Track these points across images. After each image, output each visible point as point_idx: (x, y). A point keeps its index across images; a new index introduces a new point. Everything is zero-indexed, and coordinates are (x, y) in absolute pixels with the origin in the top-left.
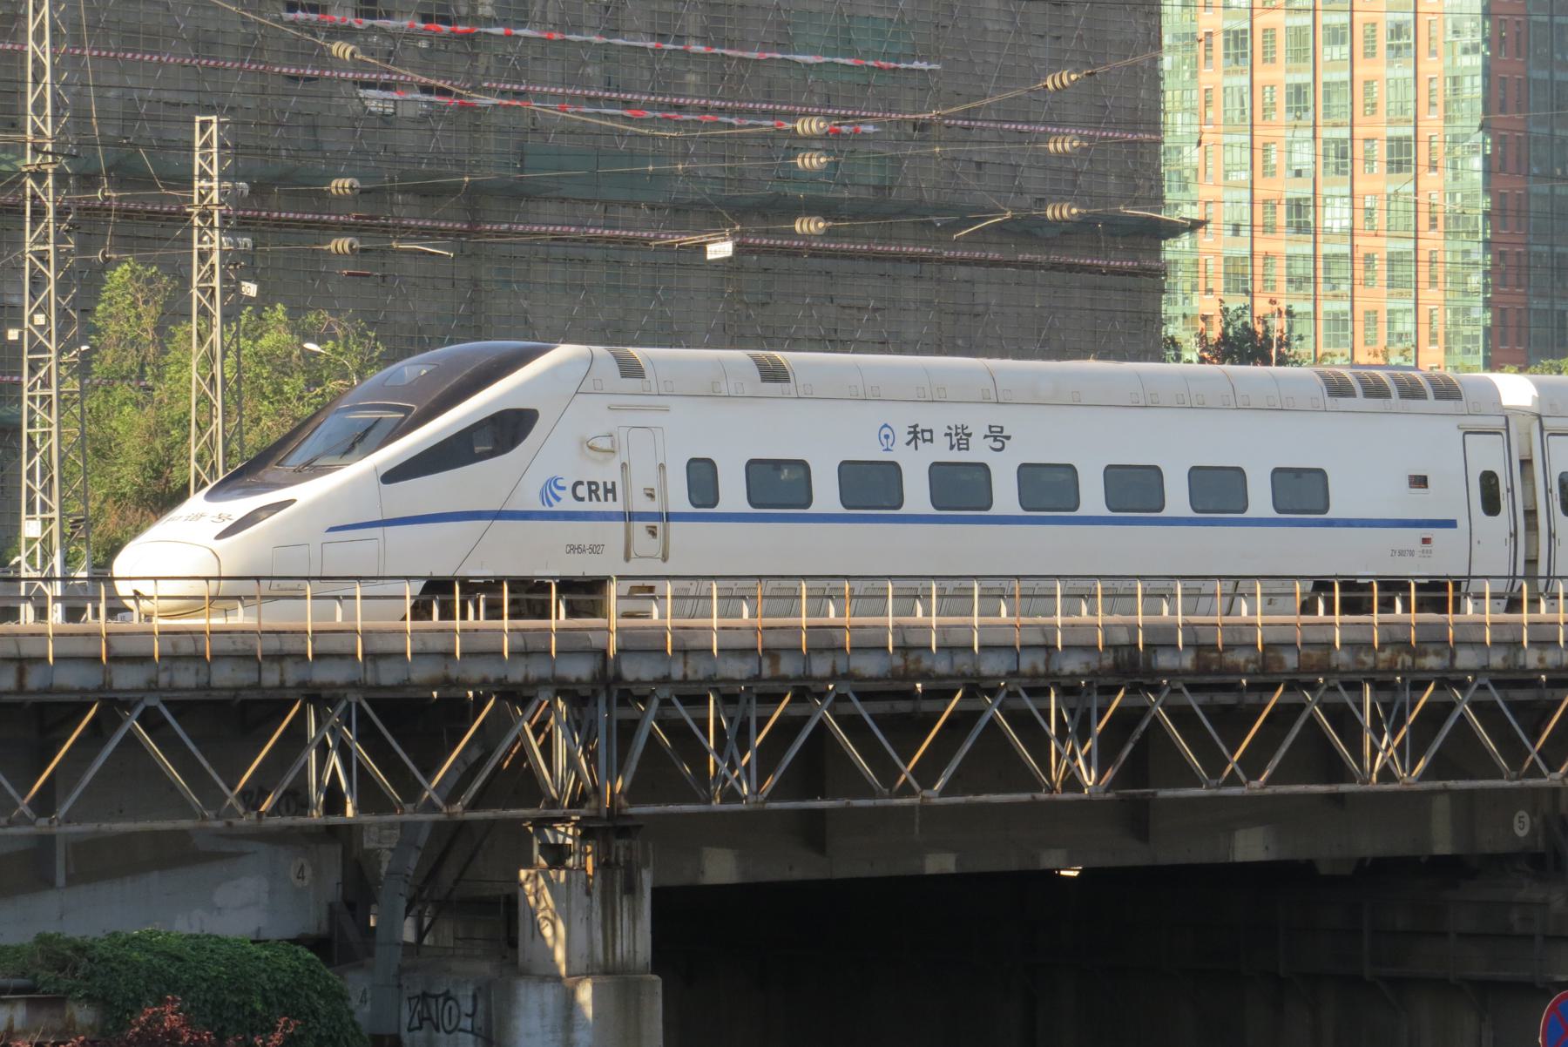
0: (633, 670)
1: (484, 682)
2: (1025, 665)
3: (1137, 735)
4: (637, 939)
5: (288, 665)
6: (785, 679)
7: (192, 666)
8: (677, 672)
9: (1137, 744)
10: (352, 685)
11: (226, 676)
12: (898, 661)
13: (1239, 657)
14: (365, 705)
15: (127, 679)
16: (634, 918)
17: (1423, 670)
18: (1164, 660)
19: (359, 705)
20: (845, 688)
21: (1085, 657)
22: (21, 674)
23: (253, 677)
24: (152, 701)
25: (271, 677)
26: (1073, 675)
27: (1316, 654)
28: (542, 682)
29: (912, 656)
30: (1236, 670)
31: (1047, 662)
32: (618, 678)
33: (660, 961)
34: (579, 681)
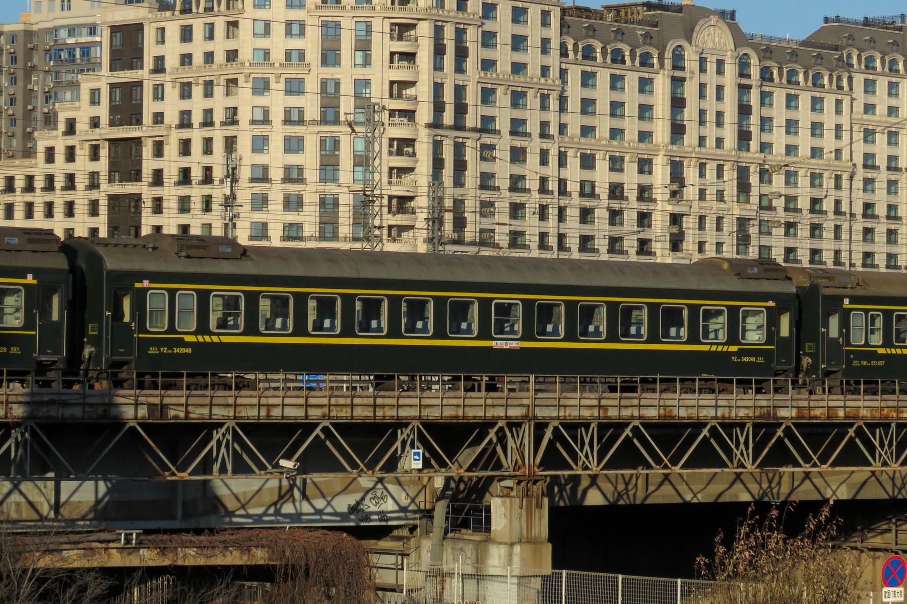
0: (541, 413)
1: (475, 417)
2: (719, 414)
3: (770, 445)
4: (542, 527)
5: (387, 409)
6: (610, 418)
7: (344, 410)
8: (562, 414)
9: (771, 449)
10: (414, 418)
11: (358, 412)
12: (662, 412)
13: (818, 412)
14: (421, 426)
15: (314, 413)
16: (540, 519)
17: (901, 419)
18: (783, 413)
19: (418, 427)
20: (637, 423)
21: (747, 411)
22: (268, 411)
23: (371, 414)
24: (326, 423)
25: (380, 413)
26: (741, 418)
27: (853, 412)
28: (499, 418)
29: (668, 409)
30: (816, 418)
31: (730, 413)
32: (535, 417)
33: (553, 537)
34: (516, 417)
